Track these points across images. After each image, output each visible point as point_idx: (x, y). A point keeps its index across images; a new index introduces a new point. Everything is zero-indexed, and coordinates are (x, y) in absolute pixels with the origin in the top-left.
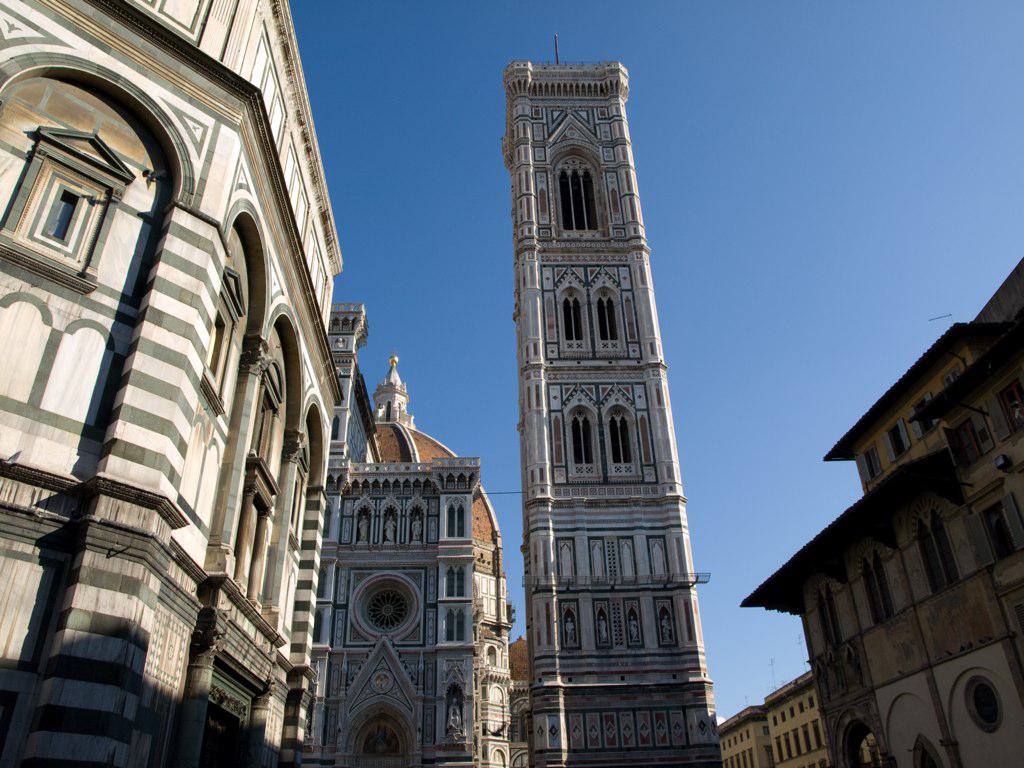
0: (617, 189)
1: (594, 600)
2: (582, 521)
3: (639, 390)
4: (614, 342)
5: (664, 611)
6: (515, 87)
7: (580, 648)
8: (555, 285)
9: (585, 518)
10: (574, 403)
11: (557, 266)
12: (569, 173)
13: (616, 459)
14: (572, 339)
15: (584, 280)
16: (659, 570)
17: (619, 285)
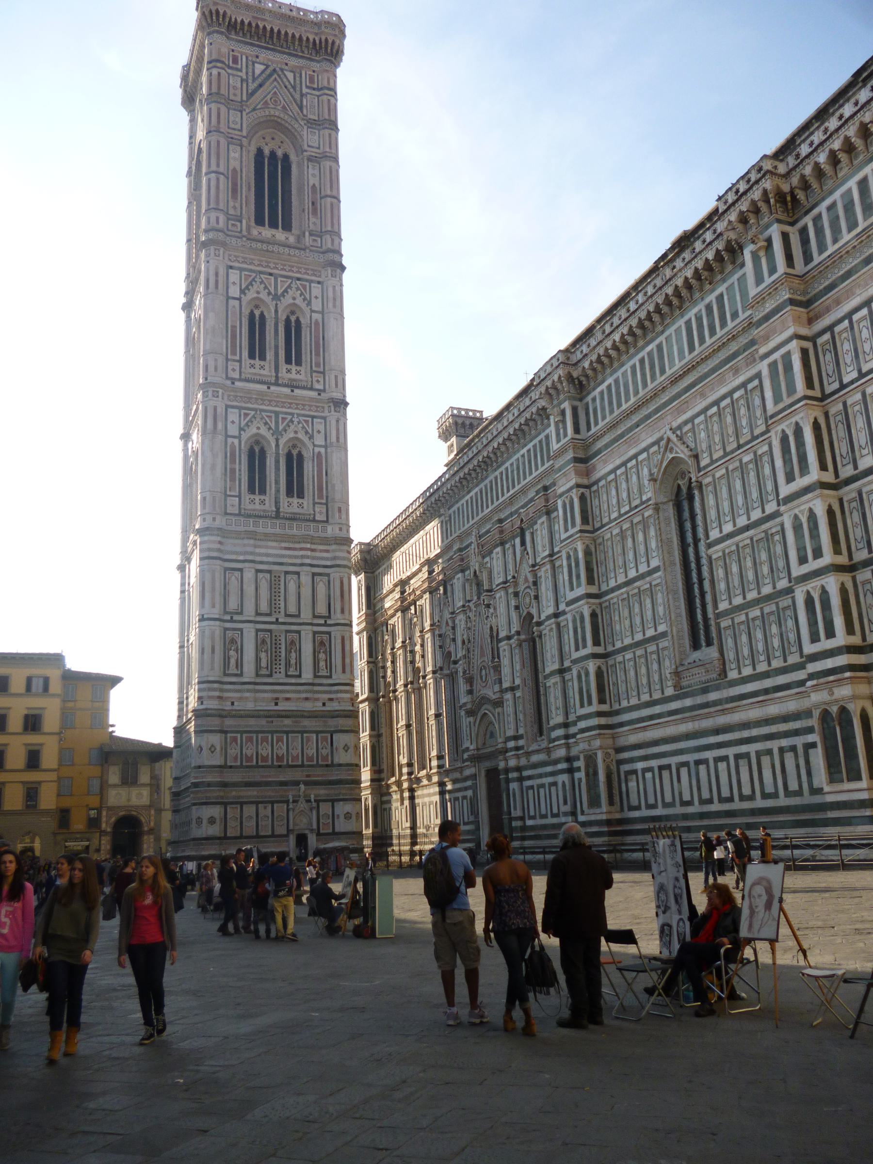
0: (317, 185)
1: (257, 631)
2: (252, 553)
3: (319, 425)
4: (298, 368)
5: (322, 643)
6: (212, 16)
7: (241, 675)
8: (242, 292)
9: (258, 550)
10: (253, 430)
12: (267, 152)
13: (289, 493)
14: (254, 358)
15: (273, 292)
16: (322, 609)
17: (309, 304)
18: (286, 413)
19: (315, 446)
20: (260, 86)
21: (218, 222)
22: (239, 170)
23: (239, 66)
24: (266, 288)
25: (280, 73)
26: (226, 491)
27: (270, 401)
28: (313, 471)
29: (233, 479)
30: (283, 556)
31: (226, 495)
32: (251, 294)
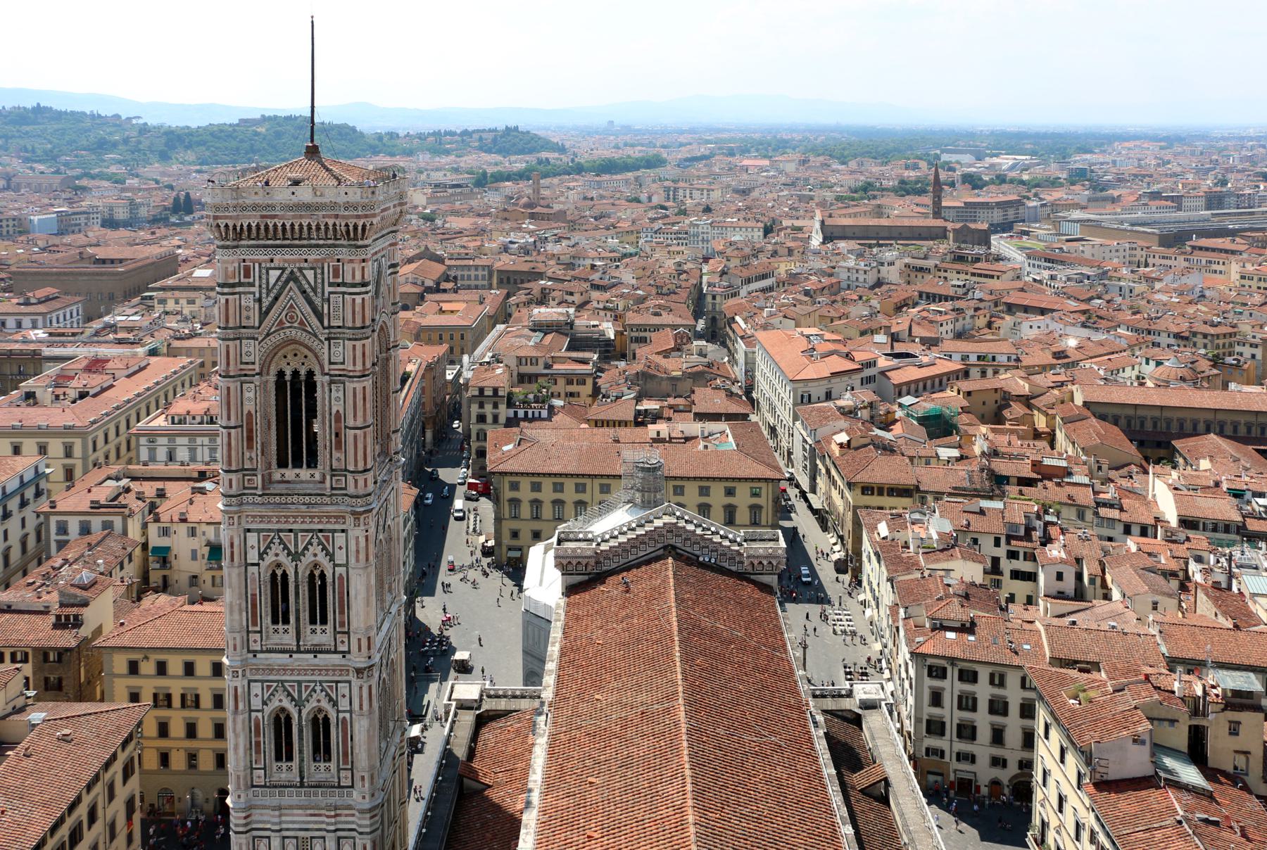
0: (342, 412)
9: (284, 818)
10: (275, 704)
11: (263, 530)
17: (332, 559)
18: (309, 681)
20: (276, 299)
21: (231, 486)
22: (253, 412)
23: (251, 280)
24: (284, 550)
25: (298, 274)
26: (251, 764)
27: (292, 670)
28: (338, 737)
29: (258, 752)
30: (309, 822)
31: (252, 769)
32: (270, 559)
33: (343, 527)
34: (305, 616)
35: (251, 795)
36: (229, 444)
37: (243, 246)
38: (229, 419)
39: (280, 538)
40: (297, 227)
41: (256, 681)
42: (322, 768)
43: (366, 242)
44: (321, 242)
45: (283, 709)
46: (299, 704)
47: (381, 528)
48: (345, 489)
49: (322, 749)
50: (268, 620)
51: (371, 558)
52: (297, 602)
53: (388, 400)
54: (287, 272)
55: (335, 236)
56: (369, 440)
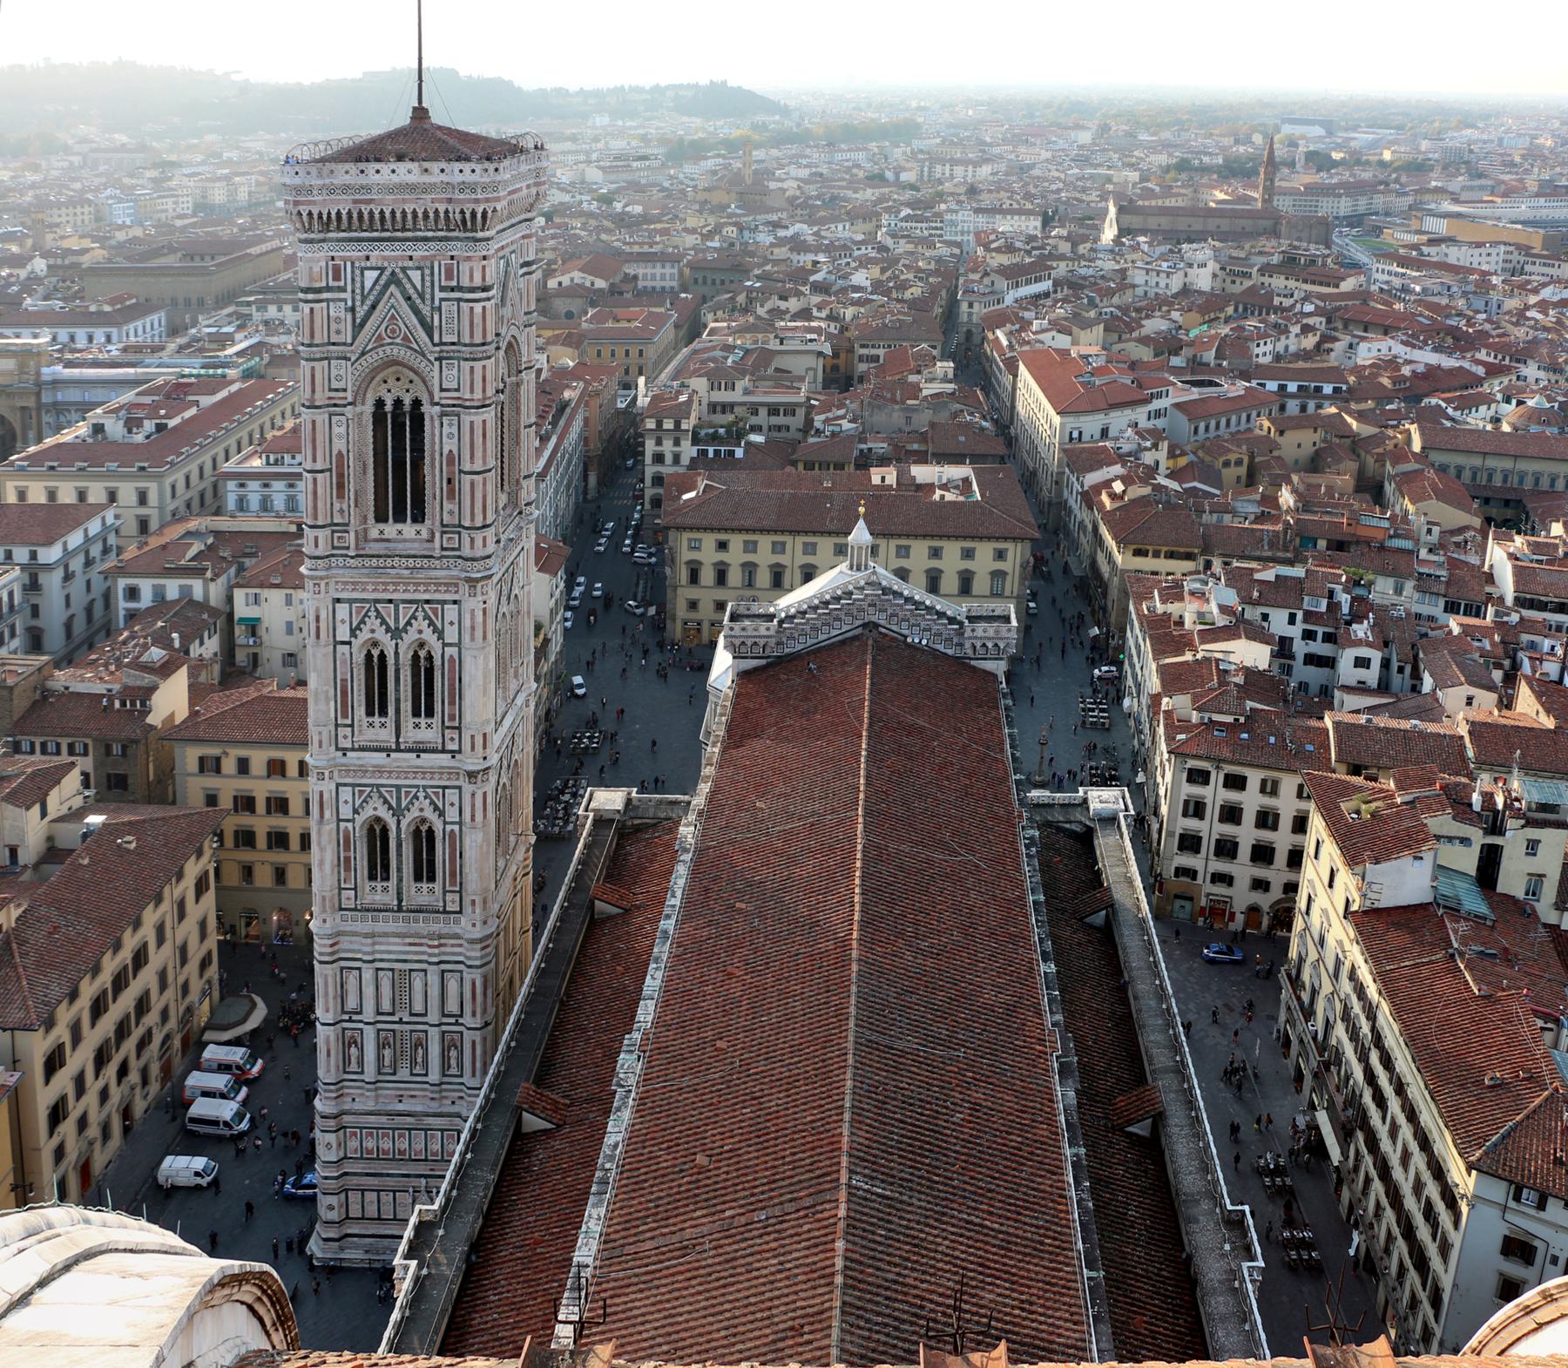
0: (455, 452)
3: (452, 795)
10: (368, 812)
13: (418, 878)
17: (441, 637)
19: (445, 823)
20: (374, 307)
23: (342, 283)
29: (347, 869)
31: (340, 889)
32: (364, 635)
33: (456, 597)
34: (407, 706)
35: (338, 920)
36: (315, 493)
37: (331, 240)
38: (314, 460)
39: (377, 610)
40: (398, 215)
41: (345, 785)
42: (425, 890)
43: (487, 234)
44: (430, 234)
45: (378, 819)
46: (398, 813)
47: (504, 599)
48: (459, 549)
49: (425, 870)
50: (360, 711)
51: (490, 635)
52: (397, 690)
53: (518, 436)
54: (387, 273)
55: (447, 225)
56: (490, 488)
